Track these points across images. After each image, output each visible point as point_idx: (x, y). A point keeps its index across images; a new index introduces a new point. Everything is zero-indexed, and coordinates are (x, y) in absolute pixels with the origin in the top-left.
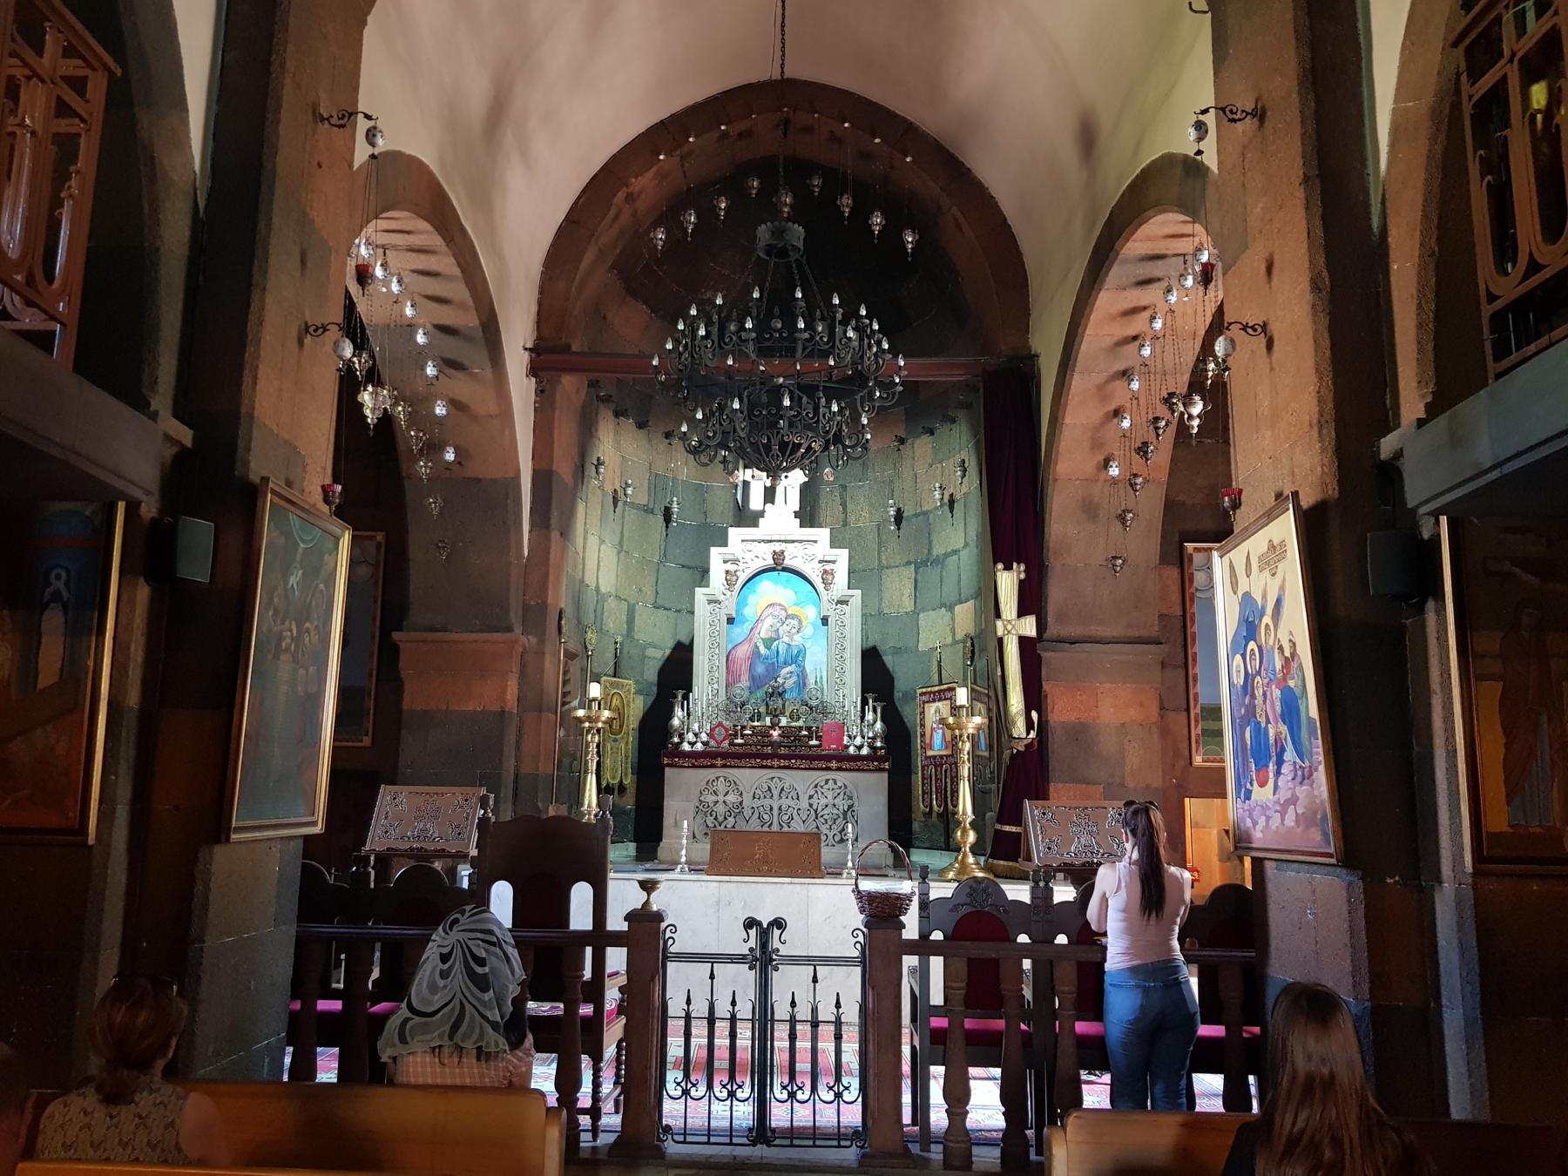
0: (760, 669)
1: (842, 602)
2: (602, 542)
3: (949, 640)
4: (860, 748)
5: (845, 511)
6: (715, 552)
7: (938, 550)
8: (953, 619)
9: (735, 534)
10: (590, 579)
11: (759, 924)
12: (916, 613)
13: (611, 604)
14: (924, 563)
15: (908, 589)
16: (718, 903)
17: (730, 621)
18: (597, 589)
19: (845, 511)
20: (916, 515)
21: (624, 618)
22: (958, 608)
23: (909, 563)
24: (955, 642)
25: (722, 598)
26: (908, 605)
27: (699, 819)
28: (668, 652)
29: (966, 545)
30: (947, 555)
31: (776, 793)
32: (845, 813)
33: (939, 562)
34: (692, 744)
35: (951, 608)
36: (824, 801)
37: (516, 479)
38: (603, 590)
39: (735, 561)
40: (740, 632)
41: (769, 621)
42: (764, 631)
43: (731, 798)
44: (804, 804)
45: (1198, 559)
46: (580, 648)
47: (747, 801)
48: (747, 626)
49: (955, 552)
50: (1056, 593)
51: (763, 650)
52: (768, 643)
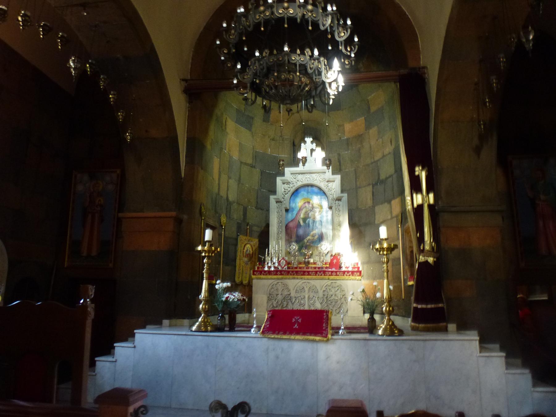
0: (301, 232)
1: (339, 199)
2: (229, 178)
3: (389, 217)
5: (340, 165)
6: (279, 180)
7: (383, 177)
8: (391, 207)
10: (223, 193)
11: (224, 407)
12: (374, 207)
13: (235, 206)
14: (376, 184)
15: (370, 196)
16: (268, 349)
17: (287, 211)
18: (227, 199)
19: (340, 165)
20: (372, 163)
21: (242, 213)
22: (393, 202)
23: (369, 185)
24: (392, 218)
26: (370, 202)
28: (263, 228)
30: (387, 178)
31: (306, 289)
33: (383, 182)
34: (270, 267)
35: (389, 202)
36: (331, 293)
37: (174, 140)
38: (231, 199)
39: (288, 183)
40: (290, 216)
42: (302, 216)
43: (286, 293)
44: (321, 294)
46: (218, 225)
47: (293, 294)
48: (295, 213)
49: (391, 176)
52: (305, 220)
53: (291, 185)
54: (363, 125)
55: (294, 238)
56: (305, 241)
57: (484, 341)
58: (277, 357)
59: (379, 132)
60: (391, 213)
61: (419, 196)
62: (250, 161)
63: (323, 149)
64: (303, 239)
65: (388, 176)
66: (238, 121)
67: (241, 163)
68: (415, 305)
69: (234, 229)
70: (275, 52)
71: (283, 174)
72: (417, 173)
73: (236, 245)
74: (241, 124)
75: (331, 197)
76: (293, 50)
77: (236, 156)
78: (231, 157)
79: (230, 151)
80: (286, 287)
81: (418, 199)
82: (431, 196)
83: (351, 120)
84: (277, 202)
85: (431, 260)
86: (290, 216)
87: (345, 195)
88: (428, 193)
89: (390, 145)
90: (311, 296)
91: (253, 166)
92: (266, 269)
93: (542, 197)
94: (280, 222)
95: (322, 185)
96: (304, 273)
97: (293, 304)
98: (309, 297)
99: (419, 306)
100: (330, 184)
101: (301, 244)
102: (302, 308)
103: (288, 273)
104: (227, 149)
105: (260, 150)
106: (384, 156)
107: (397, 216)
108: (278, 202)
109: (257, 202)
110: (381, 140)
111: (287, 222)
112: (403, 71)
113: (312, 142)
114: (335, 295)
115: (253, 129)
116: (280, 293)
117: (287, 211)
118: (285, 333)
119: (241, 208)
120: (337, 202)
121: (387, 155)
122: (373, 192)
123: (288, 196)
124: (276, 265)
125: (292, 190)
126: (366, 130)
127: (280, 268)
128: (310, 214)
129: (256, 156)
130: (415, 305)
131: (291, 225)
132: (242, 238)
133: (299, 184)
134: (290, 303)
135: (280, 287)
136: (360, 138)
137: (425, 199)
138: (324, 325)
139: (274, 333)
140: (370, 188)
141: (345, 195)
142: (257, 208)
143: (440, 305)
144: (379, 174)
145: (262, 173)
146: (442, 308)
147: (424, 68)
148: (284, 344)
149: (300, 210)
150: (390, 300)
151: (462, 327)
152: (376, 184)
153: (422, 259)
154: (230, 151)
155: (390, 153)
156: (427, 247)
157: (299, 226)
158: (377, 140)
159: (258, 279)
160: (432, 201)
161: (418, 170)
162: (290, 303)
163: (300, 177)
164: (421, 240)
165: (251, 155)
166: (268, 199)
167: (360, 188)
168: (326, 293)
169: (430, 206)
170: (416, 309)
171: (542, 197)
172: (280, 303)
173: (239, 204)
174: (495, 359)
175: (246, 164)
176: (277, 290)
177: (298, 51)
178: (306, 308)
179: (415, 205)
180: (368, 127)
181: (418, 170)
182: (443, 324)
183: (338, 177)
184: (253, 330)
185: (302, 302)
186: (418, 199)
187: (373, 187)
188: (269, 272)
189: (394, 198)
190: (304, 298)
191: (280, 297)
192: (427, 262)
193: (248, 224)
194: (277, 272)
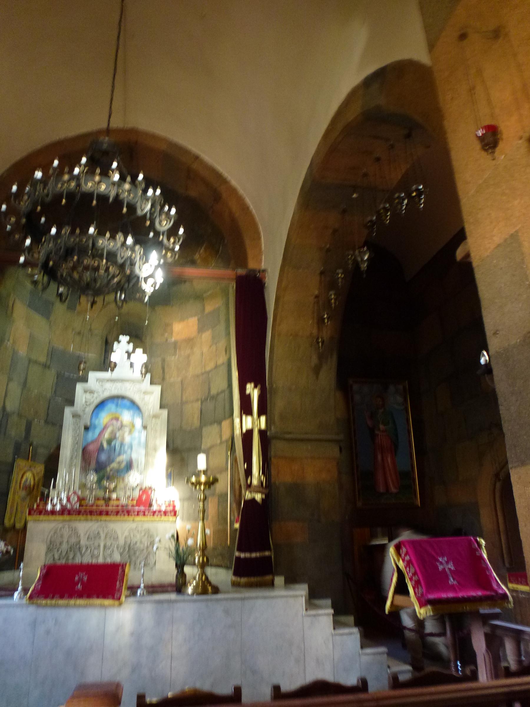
0: (103, 457)
1: (156, 416)
2: (10, 380)
3: (219, 441)
6: (79, 387)
7: (214, 392)
9: (93, 376)
12: (201, 428)
13: (14, 419)
17: (87, 428)
23: (197, 400)
24: (221, 443)
25: (81, 414)
27: (50, 555)
30: (218, 394)
31: (103, 536)
32: (147, 547)
33: (214, 398)
35: (220, 423)
39: (92, 392)
40: (91, 436)
41: (109, 430)
42: (107, 435)
43: (73, 540)
45: (355, 387)
47: (83, 542)
48: (97, 432)
50: (278, 404)
51: (105, 445)
52: (109, 442)
53: (95, 395)
54: (196, 327)
55: (93, 465)
56: (108, 469)
57: (313, 596)
58: (48, 632)
59: (213, 338)
60: (221, 437)
61: (249, 418)
62: (42, 359)
63: (144, 352)
64: (105, 467)
65: (220, 390)
66: (31, 305)
67: (30, 361)
68: (237, 554)
69: (10, 450)
70: (78, 231)
71: (85, 379)
72: (248, 392)
73: (11, 472)
74: (37, 310)
75: (146, 414)
76: (101, 233)
77: (22, 351)
78: (15, 353)
79: (14, 342)
80: (75, 532)
81: (248, 423)
82: (263, 419)
83: (182, 320)
84: (73, 416)
85: (258, 497)
86: (91, 436)
88: (259, 415)
90: (109, 544)
91: (46, 366)
92: (49, 507)
93: (381, 427)
94: (75, 443)
95: (137, 398)
96: (101, 513)
97: (82, 557)
98: (105, 547)
99: (242, 555)
100: (147, 397)
101: (101, 474)
102: (94, 561)
103: (79, 513)
104: (11, 341)
105: (59, 345)
107: (227, 441)
108: (76, 416)
109: (48, 414)
111: (85, 444)
112: (241, 271)
113: (129, 343)
114: (141, 542)
115: (52, 318)
116: (65, 540)
117: (87, 428)
118: (62, 597)
119: (24, 422)
120: (154, 419)
123: (89, 410)
124: (65, 501)
125: (97, 401)
126: (199, 332)
127: (69, 506)
128: (118, 435)
129: (52, 353)
130: (237, 554)
131: (91, 448)
132: (21, 463)
133: (107, 394)
134: (78, 554)
135: (66, 532)
136: (190, 341)
137: (256, 423)
138: (118, 583)
139: (46, 597)
140: (198, 405)
141: (165, 412)
142: (46, 422)
143: (267, 553)
144: (209, 389)
145: (59, 376)
146: (269, 558)
147: (264, 271)
148: (61, 613)
149: (105, 428)
150: (204, 548)
151: (291, 580)
152: (206, 399)
153: (248, 495)
154: (14, 342)
155: (223, 364)
156: (255, 482)
157: (101, 449)
158: (211, 346)
159: (35, 521)
160: (263, 426)
161: (249, 387)
162: (78, 554)
163: (108, 385)
164: (249, 472)
165: (45, 351)
166: (62, 413)
167: (187, 402)
169: (261, 432)
170: (238, 559)
171: (381, 427)
172: (64, 554)
173: (20, 416)
174: (321, 618)
175: (36, 362)
176: (62, 536)
177: (108, 235)
178: (101, 560)
179: (244, 430)
180: (201, 330)
181: (249, 387)
182: (269, 578)
183: (157, 389)
184: (16, 594)
185: (96, 552)
186: (248, 423)
187: (202, 403)
188: (53, 512)
190: (99, 546)
191: (65, 547)
192: (253, 500)
193: (31, 444)
194: (64, 511)
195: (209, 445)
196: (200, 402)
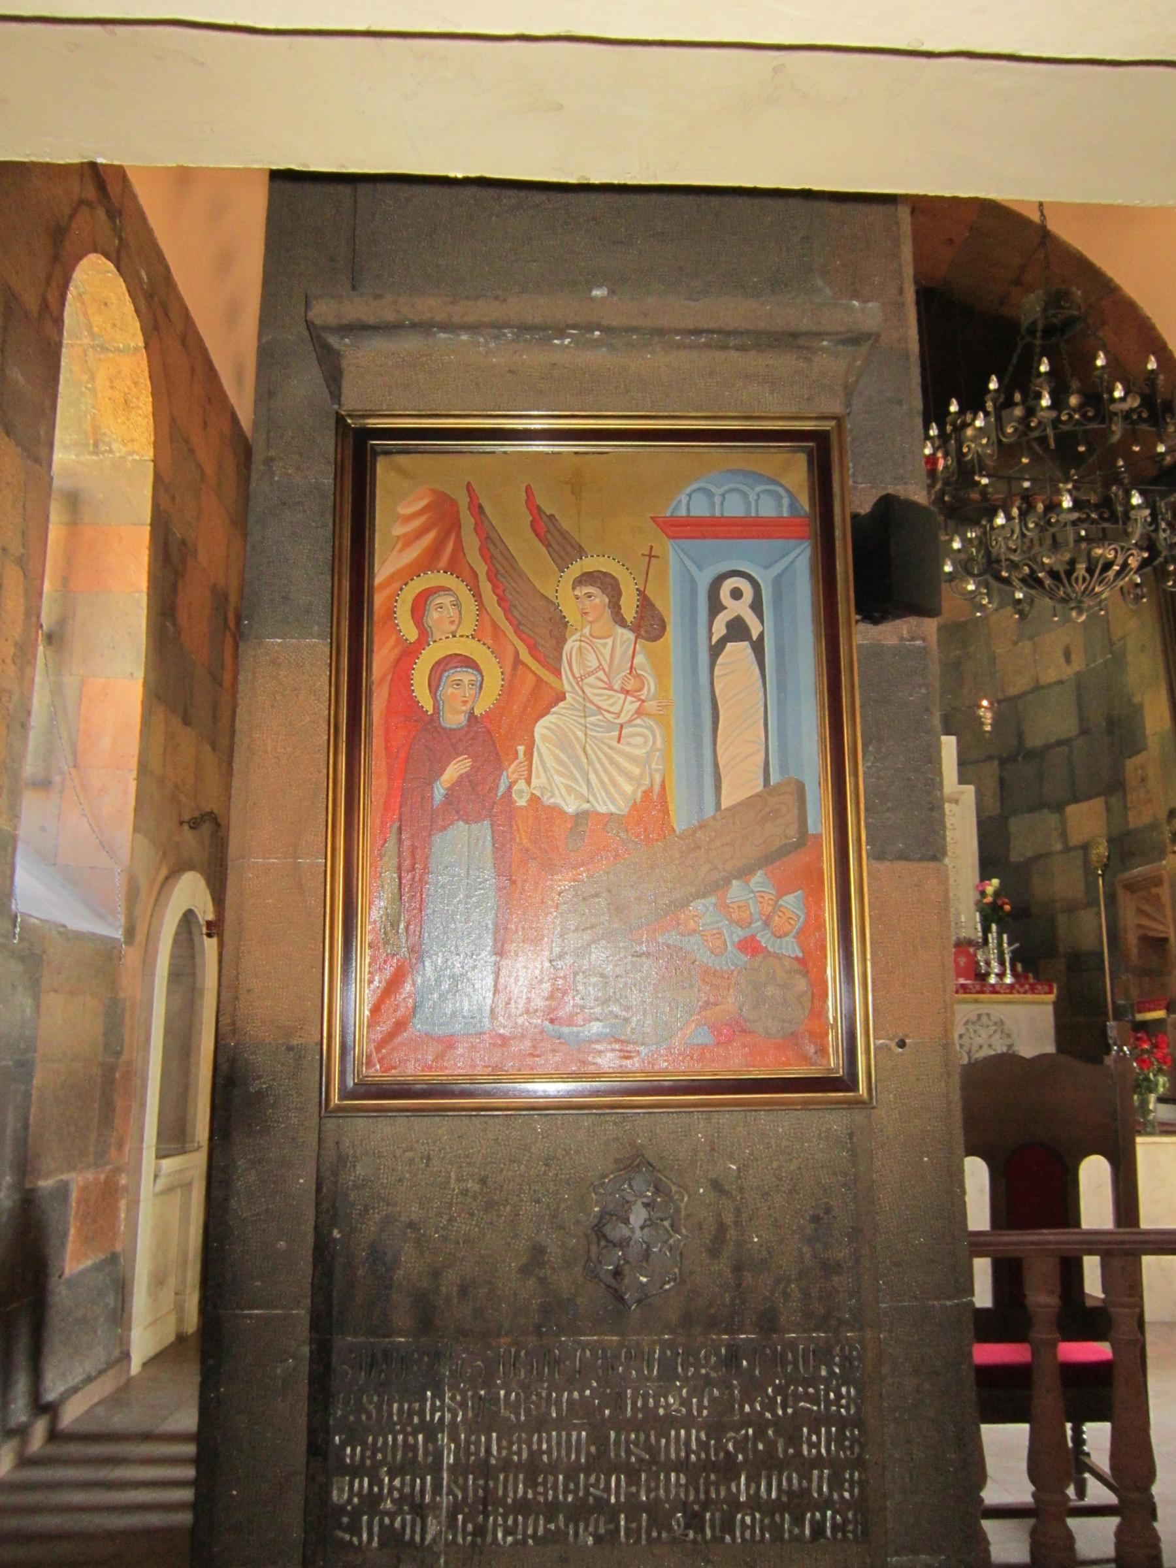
3: (1058, 847)
4: (1001, 976)
7: (1034, 741)
8: (1063, 822)
14: (1013, 758)
22: (1071, 809)
23: (990, 758)
24: (1067, 849)
29: (1084, 732)
30: (1049, 747)
35: (1059, 808)
36: (979, 1041)
49: (1060, 743)
60: (1064, 836)
65: (1052, 740)
87: (971, 789)
89: (1062, 660)
106: (1037, 688)
107: (1085, 848)
110: (1028, 644)
114: (990, 1046)
121: (1050, 686)
122: (1002, 780)
141: (971, 789)
144: (1020, 736)
152: (1013, 758)
155: (1061, 682)
158: (1015, 643)
168: (966, 1041)
187: (1003, 762)
189: (1076, 800)
195: (1029, 854)
196: (996, 763)
